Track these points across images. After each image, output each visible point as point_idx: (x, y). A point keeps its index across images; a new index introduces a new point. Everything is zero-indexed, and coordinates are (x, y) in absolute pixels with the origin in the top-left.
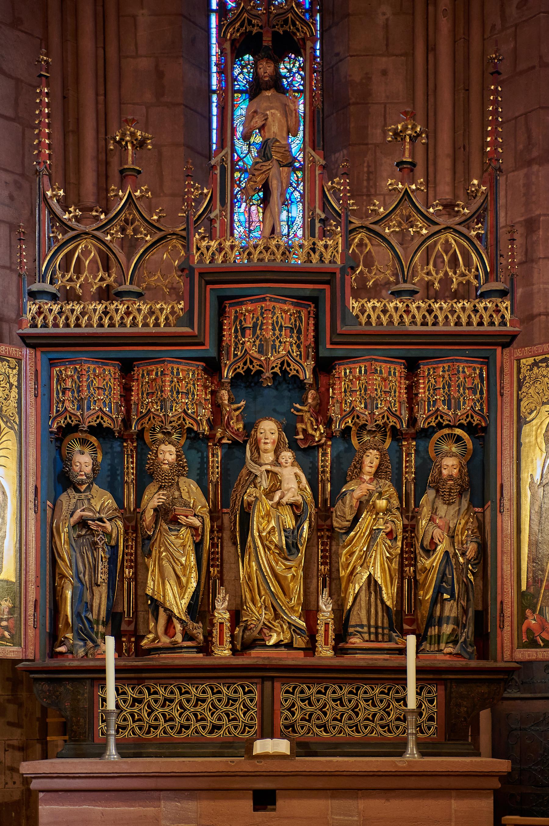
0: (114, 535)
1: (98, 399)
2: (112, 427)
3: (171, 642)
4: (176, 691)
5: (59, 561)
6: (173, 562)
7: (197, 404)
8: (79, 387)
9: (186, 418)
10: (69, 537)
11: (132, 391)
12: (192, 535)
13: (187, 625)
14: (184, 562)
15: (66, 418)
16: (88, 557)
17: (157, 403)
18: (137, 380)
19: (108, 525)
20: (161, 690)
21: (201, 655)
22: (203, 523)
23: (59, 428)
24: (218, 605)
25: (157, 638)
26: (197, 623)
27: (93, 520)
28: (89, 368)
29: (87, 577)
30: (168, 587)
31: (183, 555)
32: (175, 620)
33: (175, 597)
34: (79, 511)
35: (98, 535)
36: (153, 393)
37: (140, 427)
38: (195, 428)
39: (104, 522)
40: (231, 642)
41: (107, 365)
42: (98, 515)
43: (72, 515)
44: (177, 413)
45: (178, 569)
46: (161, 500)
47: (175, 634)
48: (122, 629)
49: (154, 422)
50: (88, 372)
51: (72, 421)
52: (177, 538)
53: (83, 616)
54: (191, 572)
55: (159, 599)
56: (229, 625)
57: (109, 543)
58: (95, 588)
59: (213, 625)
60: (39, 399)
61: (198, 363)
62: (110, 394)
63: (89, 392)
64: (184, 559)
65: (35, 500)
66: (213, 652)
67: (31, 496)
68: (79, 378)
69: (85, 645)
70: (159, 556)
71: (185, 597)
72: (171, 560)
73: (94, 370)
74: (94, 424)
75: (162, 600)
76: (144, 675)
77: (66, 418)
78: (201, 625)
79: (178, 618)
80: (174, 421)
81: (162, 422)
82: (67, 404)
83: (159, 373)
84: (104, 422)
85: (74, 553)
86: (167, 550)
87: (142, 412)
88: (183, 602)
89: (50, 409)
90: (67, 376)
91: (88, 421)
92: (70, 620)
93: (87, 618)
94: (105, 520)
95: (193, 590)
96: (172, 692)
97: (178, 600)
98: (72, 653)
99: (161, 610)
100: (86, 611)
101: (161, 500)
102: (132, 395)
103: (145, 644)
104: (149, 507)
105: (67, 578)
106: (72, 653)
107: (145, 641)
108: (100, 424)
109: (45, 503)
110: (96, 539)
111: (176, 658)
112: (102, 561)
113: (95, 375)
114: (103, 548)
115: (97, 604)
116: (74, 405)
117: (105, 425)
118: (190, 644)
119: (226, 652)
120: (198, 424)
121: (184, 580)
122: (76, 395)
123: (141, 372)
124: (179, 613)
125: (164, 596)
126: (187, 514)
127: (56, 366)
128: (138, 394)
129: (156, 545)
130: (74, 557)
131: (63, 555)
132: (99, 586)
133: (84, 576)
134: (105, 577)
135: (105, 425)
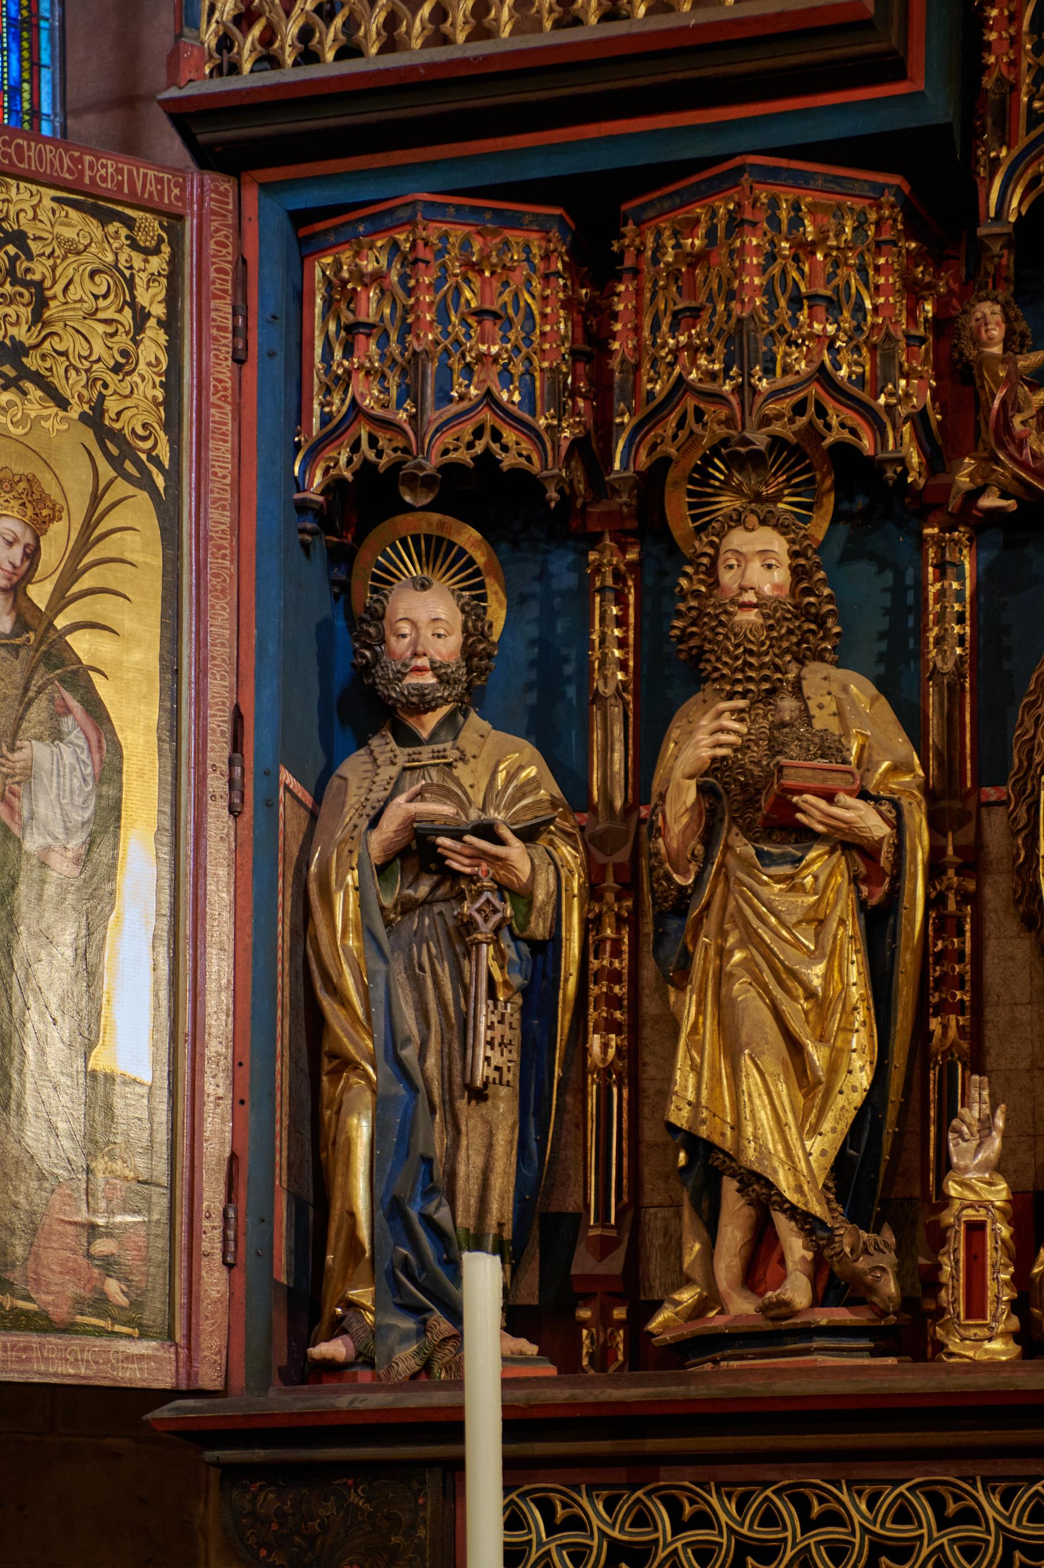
0: (540, 895)
1: (481, 357)
2: (536, 467)
3: (764, 1309)
4: (787, 1511)
5: (327, 1003)
6: (773, 986)
7: (873, 348)
8: (407, 310)
9: (831, 406)
10: (363, 904)
11: (615, 316)
12: (855, 880)
13: (831, 1241)
14: (817, 982)
15: (355, 447)
16: (437, 985)
17: (710, 349)
18: (636, 272)
19: (516, 852)
20: (725, 1511)
21: (891, 1361)
22: (898, 825)
23: (334, 487)
24: (960, 1153)
25: (711, 1300)
26: (877, 1231)
27: (457, 835)
28: (444, 237)
29: (432, 1061)
30: (751, 1081)
31: (813, 957)
32: (782, 1223)
33: (780, 1125)
34: (401, 799)
35: (479, 893)
36: (695, 313)
37: (643, 459)
38: (867, 444)
39: (501, 842)
40: (1017, 1307)
41: (514, 222)
42: (474, 814)
43: (374, 823)
44: (790, 379)
45: (795, 1010)
46: (724, 738)
47: (784, 1277)
48: (575, 1271)
49: (698, 429)
50: (441, 253)
51: (380, 454)
52: (792, 889)
53: (413, 1213)
54: (847, 1029)
55: (716, 1139)
56: (1005, 1232)
57: (523, 927)
58: (461, 1104)
59: (938, 1237)
60: (250, 370)
61: (880, 178)
62: (528, 340)
63: (446, 334)
64: (820, 969)
65: (231, 763)
66: (941, 1346)
67: (218, 750)
68: (403, 278)
69: (423, 1330)
70: (721, 968)
71: (826, 1126)
72: (768, 977)
73: (466, 245)
74: (463, 456)
75: (728, 1145)
76: (652, 1445)
77: (355, 447)
78: (888, 1236)
79: (793, 1212)
80: (779, 416)
81: (729, 422)
82: (359, 385)
83: (720, 232)
84: (505, 448)
85: (381, 966)
86: (750, 938)
87: (651, 394)
88: (815, 1145)
89: (299, 414)
90: (358, 275)
91: (438, 447)
92: (364, 1233)
93: (428, 1221)
94: (505, 832)
95: (857, 1098)
96: (770, 1518)
97: (793, 1134)
98: (370, 1364)
99: (730, 1186)
100: (428, 1194)
101: (724, 738)
102: (614, 336)
103: (665, 1326)
104: (677, 774)
105: (356, 1066)
106: (370, 1364)
107: (664, 1315)
108: (487, 458)
109: (270, 775)
110: (467, 908)
111: (781, 1372)
112: (492, 994)
113: (469, 265)
114: (496, 942)
115: (476, 1173)
116: (386, 390)
117: (508, 461)
118: (841, 1315)
119: (996, 1345)
120: (879, 430)
121: (817, 1055)
122: (394, 347)
123: (650, 243)
124: (799, 1189)
125: (737, 1127)
126: (830, 785)
127: (322, 251)
128: (637, 330)
129: (710, 924)
130: (380, 981)
131: (341, 974)
132: (479, 1095)
133: (422, 1057)
134: (506, 1059)
135: (508, 461)
